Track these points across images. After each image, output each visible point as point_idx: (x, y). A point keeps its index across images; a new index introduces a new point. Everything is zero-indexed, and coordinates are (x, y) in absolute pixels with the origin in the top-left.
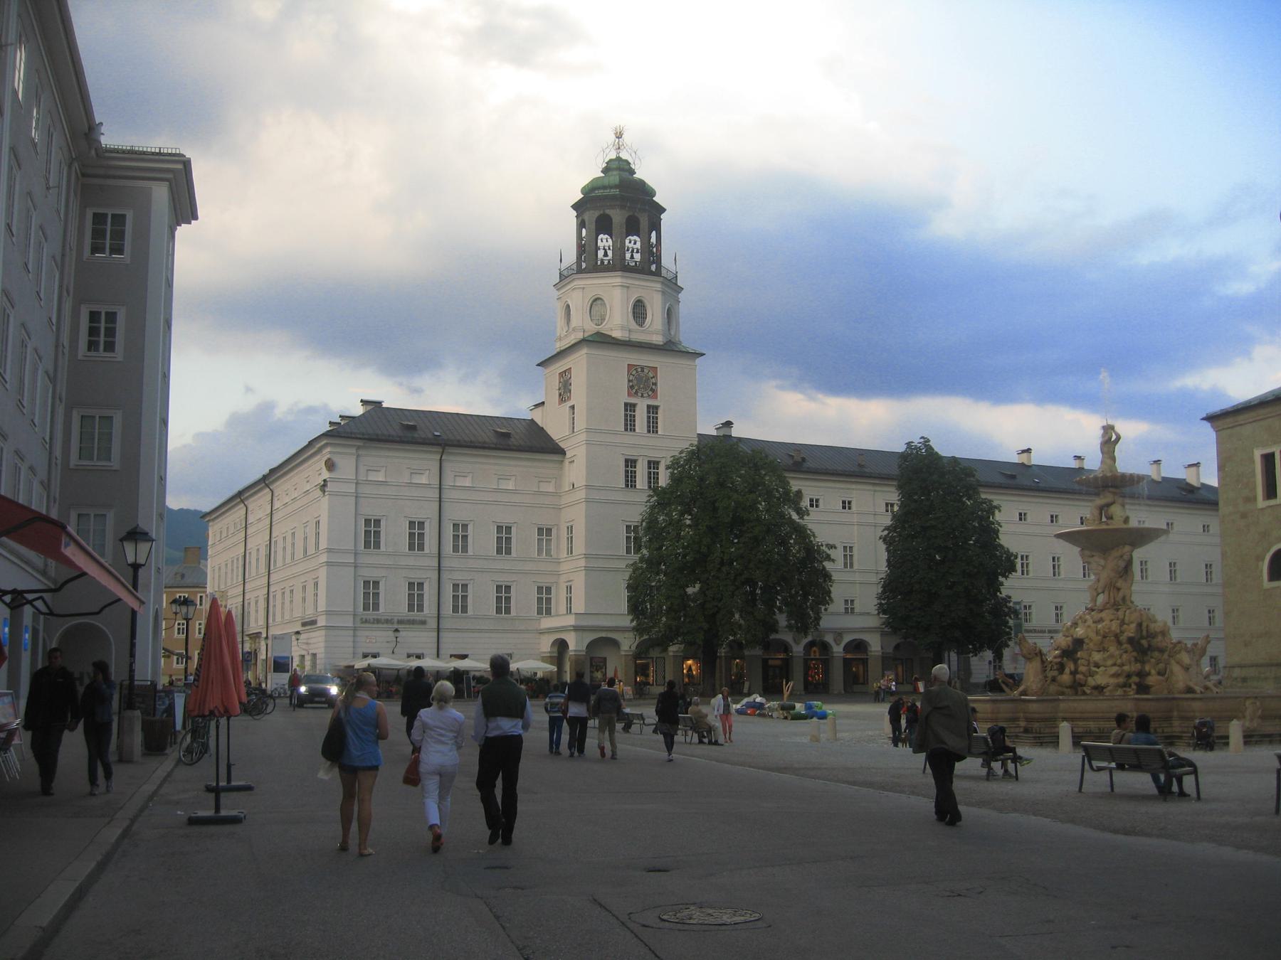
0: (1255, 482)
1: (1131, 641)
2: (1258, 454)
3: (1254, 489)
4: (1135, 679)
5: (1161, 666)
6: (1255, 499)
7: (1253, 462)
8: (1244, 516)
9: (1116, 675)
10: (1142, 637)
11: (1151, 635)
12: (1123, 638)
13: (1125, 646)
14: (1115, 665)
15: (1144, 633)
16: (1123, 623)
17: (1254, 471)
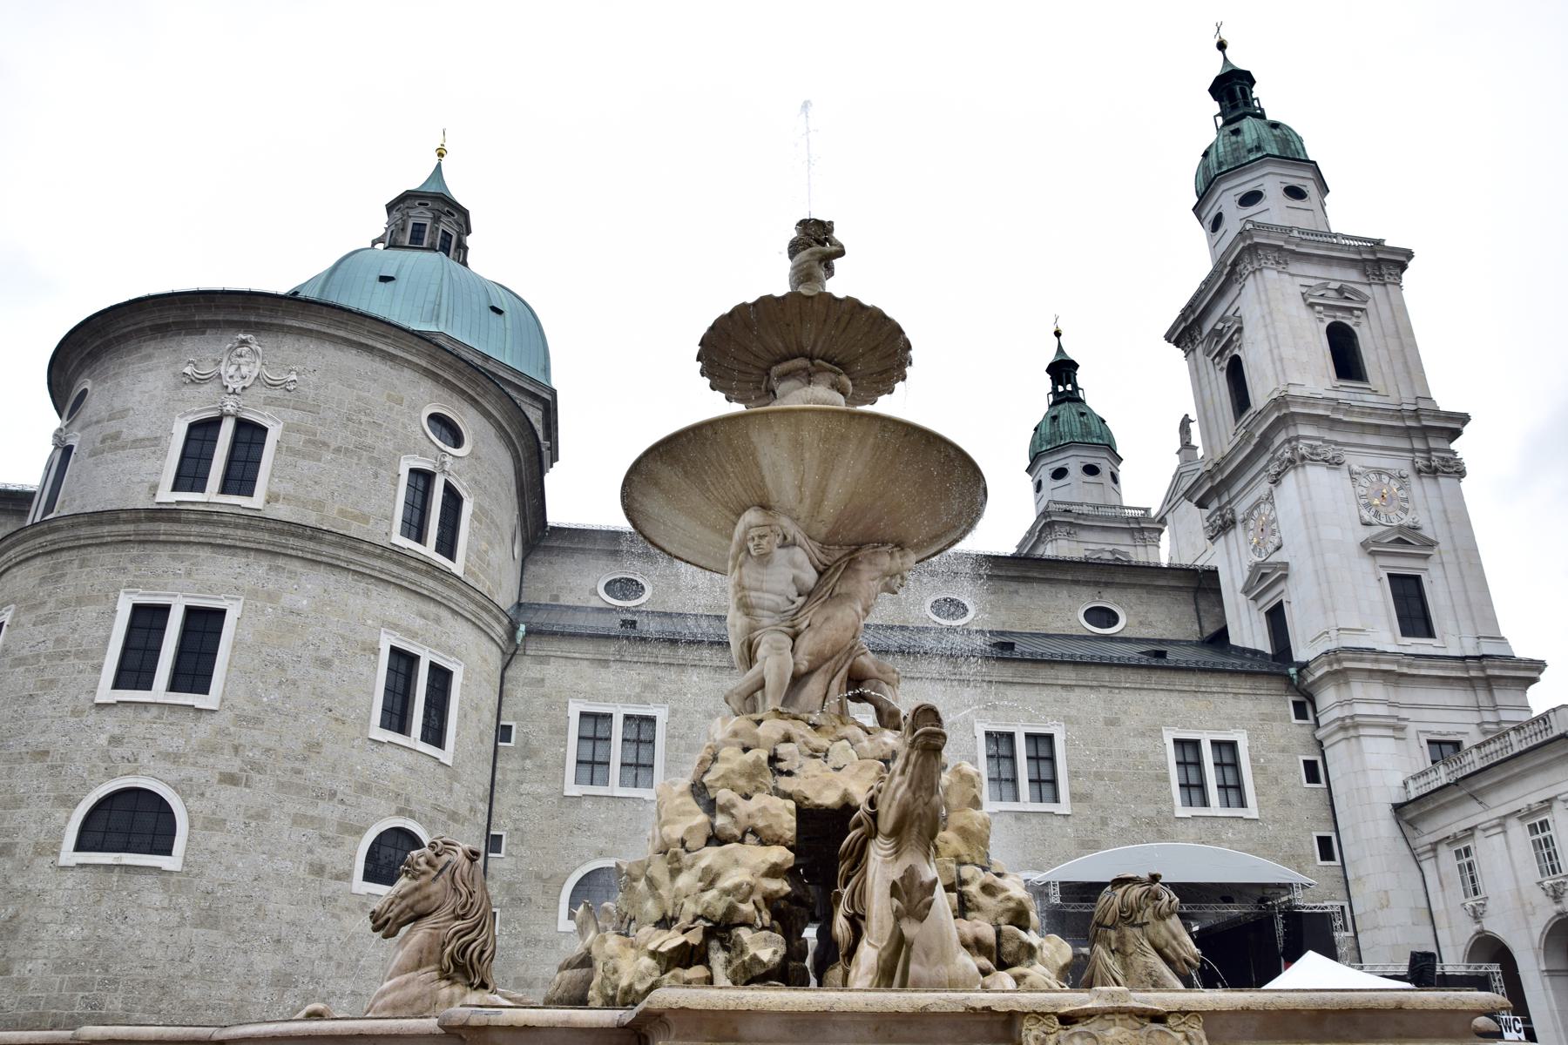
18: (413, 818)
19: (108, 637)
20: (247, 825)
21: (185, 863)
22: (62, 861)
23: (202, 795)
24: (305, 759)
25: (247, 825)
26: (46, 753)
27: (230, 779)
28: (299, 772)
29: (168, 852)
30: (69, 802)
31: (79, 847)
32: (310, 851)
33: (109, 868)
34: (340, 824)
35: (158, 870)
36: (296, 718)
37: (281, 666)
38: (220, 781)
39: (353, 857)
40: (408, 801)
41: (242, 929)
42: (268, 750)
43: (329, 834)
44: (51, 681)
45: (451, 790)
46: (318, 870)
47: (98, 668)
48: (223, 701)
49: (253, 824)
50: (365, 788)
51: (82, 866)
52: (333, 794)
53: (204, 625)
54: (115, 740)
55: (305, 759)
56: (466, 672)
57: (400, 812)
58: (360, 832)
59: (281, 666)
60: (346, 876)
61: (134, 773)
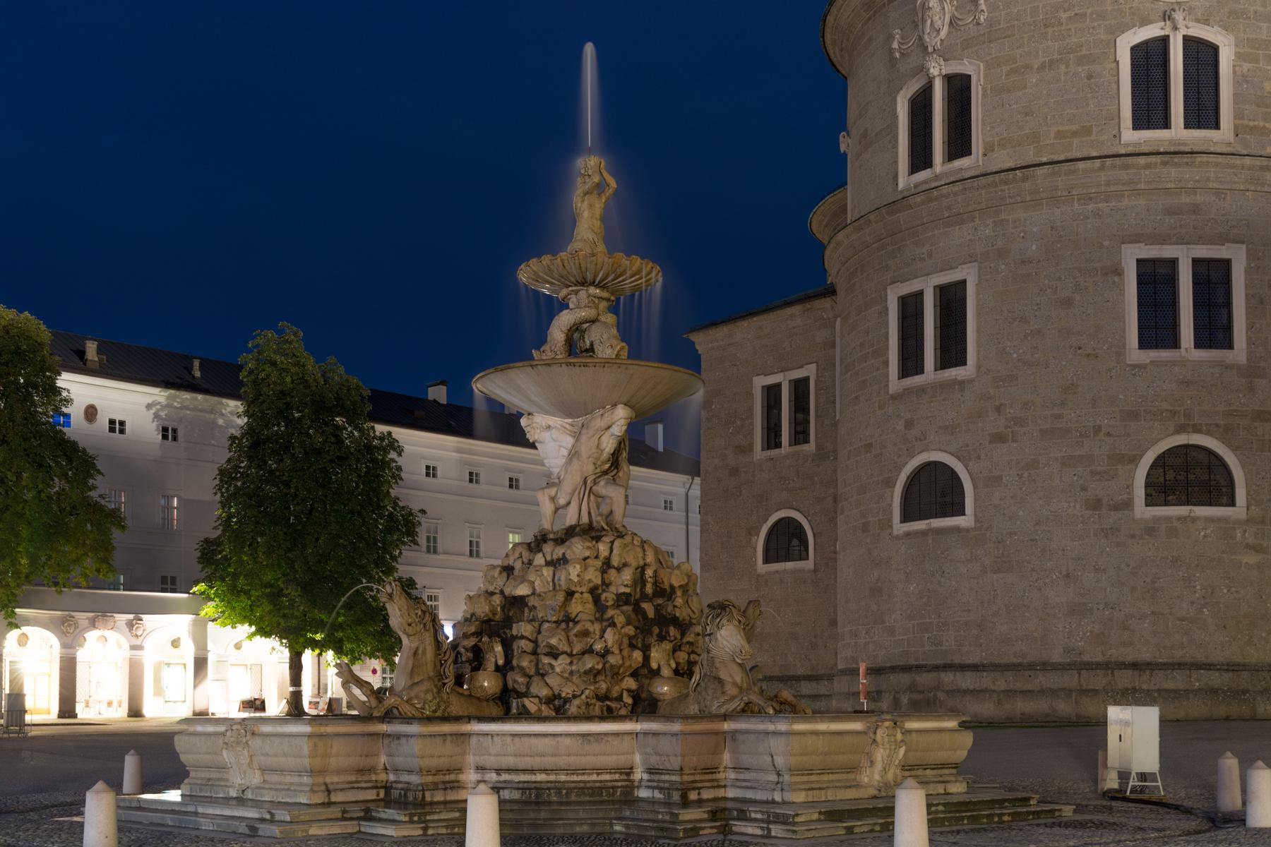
0: (751, 424)
1: (623, 600)
2: (760, 382)
3: (751, 433)
4: (630, 683)
5: (682, 656)
6: (751, 448)
7: (750, 395)
8: (734, 472)
9: (594, 674)
10: (645, 597)
11: (664, 593)
12: (608, 597)
13: (610, 613)
14: (589, 651)
15: (649, 589)
16: (607, 564)
17: (751, 409)
18: (1197, 430)
19: (887, 333)
20: (1021, 476)
21: (976, 520)
22: (895, 532)
23: (979, 457)
24: (1063, 404)
25: (1021, 476)
26: (870, 445)
27: (999, 438)
28: (1059, 416)
29: (962, 512)
30: (890, 483)
31: (906, 518)
32: (1084, 489)
33: (924, 533)
34: (1109, 457)
35: (957, 529)
36: (1047, 366)
37: (1023, 320)
38: (990, 442)
39: (1130, 487)
40: (1188, 416)
41: (1033, 570)
42: (1026, 404)
43: (1099, 468)
44: (864, 381)
45: (1251, 389)
46: (1096, 505)
47: (886, 363)
48: (979, 367)
49: (1026, 475)
50: (1132, 415)
51: (908, 534)
52: (1097, 430)
53: (952, 301)
54: (909, 424)
55: (1063, 404)
56: (1251, 255)
57: (1180, 430)
58: (1135, 459)
59: (1023, 320)
60: (1128, 504)
61: (926, 449)
